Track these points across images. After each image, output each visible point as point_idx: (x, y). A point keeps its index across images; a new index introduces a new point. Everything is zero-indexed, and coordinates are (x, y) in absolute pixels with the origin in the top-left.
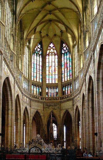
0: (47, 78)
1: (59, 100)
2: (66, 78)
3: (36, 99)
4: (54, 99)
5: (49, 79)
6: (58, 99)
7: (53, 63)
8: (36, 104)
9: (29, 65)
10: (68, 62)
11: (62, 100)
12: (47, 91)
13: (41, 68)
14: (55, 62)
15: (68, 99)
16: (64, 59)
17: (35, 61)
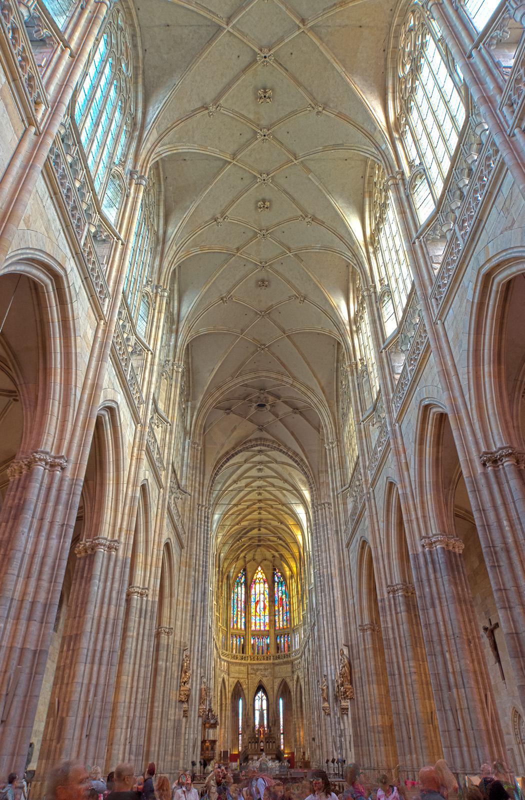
0: (253, 621)
1: (271, 661)
2: (281, 623)
3: (237, 661)
4: (264, 659)
5: (255, 623)
6: (270, 659)
7: (262, 596)
8: (237, 668)
9: (227, 605)
10: (284, 597)
11: (276, 661)
12: (252, 642)
13: (243, 606)
14: (264, 594)
15: (285, 660)
16: (278, 591)
17: (235, 595)
